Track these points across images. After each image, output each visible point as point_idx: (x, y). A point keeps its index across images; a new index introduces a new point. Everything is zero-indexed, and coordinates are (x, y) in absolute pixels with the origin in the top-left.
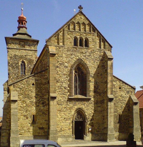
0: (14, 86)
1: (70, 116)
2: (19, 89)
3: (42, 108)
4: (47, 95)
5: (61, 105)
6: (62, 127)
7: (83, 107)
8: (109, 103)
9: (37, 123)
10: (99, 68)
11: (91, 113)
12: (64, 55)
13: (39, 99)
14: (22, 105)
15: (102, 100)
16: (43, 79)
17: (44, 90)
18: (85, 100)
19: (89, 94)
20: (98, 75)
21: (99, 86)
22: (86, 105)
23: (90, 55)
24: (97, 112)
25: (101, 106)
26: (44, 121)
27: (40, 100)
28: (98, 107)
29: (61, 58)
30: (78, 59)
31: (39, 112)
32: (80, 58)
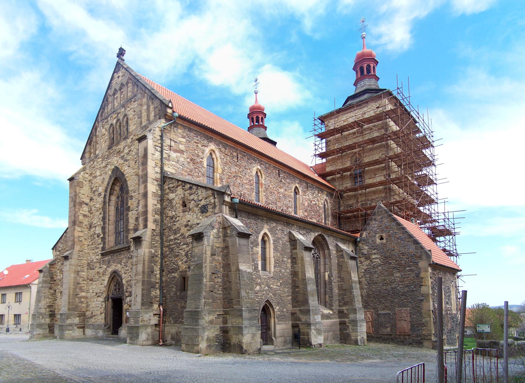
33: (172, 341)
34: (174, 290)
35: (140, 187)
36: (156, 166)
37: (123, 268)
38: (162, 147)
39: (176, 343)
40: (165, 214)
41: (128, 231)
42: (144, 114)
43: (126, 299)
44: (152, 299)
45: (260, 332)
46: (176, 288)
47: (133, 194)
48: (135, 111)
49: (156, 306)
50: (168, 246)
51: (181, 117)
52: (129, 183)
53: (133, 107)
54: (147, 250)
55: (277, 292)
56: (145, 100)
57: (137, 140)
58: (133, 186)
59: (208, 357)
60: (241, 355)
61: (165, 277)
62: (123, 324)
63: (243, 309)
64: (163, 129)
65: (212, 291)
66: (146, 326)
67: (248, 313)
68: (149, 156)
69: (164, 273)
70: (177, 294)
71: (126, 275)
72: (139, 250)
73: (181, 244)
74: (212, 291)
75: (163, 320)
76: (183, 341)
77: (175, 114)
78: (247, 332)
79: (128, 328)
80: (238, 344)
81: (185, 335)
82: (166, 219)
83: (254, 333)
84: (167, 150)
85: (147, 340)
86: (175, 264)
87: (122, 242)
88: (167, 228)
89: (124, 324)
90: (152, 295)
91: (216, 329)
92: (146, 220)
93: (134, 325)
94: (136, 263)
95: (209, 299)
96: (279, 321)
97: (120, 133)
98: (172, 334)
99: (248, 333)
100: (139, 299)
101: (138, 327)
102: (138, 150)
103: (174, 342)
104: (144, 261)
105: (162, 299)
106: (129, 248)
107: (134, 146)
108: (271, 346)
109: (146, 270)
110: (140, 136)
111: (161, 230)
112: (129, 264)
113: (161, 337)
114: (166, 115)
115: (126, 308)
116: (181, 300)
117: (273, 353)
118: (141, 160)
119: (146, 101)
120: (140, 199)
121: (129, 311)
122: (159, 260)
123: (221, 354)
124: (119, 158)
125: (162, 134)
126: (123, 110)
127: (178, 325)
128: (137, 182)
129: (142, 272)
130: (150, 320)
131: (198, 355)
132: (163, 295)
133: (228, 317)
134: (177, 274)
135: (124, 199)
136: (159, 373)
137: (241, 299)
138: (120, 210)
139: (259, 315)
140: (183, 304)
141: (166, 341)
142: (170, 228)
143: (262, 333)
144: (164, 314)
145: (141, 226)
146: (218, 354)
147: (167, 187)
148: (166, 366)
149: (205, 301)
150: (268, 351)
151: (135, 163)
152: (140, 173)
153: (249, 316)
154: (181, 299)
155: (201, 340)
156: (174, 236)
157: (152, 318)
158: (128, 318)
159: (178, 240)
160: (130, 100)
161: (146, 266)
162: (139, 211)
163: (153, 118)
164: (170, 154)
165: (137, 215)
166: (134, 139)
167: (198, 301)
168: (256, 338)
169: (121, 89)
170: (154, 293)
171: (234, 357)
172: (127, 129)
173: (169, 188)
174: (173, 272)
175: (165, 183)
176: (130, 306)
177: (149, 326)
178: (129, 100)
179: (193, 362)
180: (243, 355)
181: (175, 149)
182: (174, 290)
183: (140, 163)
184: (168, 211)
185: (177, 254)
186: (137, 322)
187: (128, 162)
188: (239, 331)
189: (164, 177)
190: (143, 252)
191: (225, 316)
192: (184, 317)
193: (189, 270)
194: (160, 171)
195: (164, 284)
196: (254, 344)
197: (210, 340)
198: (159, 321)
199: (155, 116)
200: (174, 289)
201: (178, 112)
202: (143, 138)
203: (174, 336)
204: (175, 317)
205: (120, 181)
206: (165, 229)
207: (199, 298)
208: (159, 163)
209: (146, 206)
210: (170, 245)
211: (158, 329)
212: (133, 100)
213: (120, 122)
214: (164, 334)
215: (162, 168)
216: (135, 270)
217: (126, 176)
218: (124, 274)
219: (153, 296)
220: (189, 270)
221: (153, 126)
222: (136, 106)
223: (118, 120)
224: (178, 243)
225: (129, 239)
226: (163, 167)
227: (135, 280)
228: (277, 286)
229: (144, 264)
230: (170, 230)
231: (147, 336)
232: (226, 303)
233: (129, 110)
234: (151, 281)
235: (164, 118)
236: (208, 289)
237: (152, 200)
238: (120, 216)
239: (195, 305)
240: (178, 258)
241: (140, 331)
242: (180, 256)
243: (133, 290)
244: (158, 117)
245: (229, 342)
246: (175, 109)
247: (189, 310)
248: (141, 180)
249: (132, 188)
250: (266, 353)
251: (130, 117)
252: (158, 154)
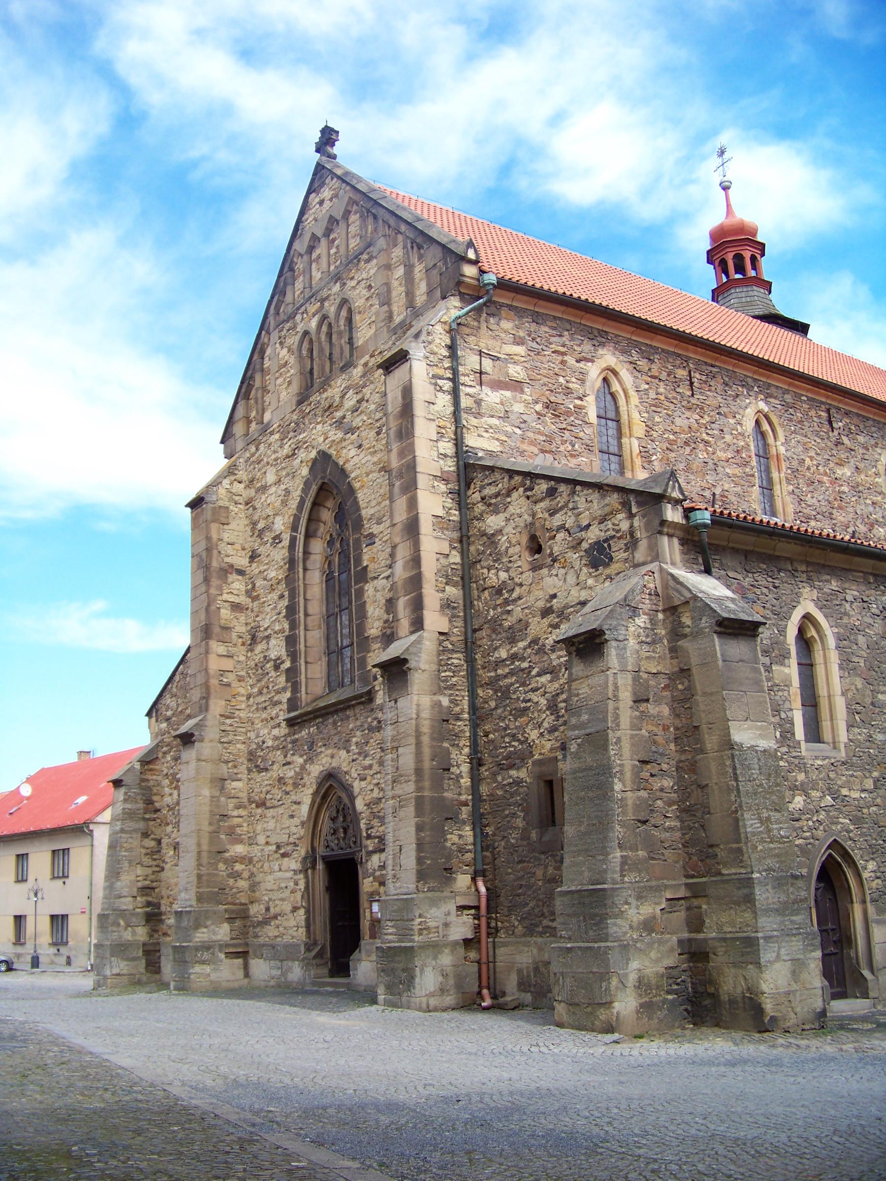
33: (523, 994)
34: (521, 825)
35: (394, 505)
36: (441, 435)
37: (353, 761)
38: (454, 380)
39: (535, 998)
40: (476, 582)
41: (364, 643)
42: (398, 292)
43: (367, 861)
44: (449, 857)
45: (818, 954)
46: (524, 819)
47: (376, 529)
48: (370, 287)
49: (463, 880)
50: (492, 683)
51: (504, 285)
52: (360, 495)
53: (364, 276)
54: (426, 701)
55: (865, 811)
56: (398, 252)
57: (379, 366)
58: (374, 503)
59: (644, 1042)
60: (757, 1035)
61: (488, 784)
62: (362, 942)
63: (756, 875)
64: (454, 326)
65: (645, 822)
66: (435, 947)
67: (773, 888)
68: (419, 410)
69: (483, 769)
70: (529, 838)
71: (363, 784)
72: (401, 703)
73: (534, 672)
74: (645, 822)
75: (488, 924)
76: (560, 992)
77: (486, 276)
78: (774, 955)
79: (379, 954)
80: (744, 997)
81: (562, 974)
82: (479, 597)
83: (797, 957)
84: (470, 386)
85: (442, 991)
86: (519, 740)
87: (347, 680)
88: (486, 626)
89: (366, 941)
90: (448, 844)
91: (665, 948)
92: (418, 605)
93: (396, 944)
94: (395, 744)
95: (637, 850)
96: (880, 911)
97: (331, 354)
98: (519, 971)
99: (778, 956)
100: (409, 860)
101: (409, 951)
102: (385, 395)
103: (528, 998)
104: (418, 734)
105: (484, 857)
106: (369, 697)
107: (372, 386)
108: (858, 1001)
109: (427, 765)
110: (388, 355)
111: (466, 634)
112: (372, 749)
113: (484, 983)
114: (459, 283)
115: (370, 890)
116: (543, 857)
117: (870, 1026)
118: (393, 424)
119: (401, 254)
120: (397, 540)
121: (378, 901)
122: (467, 729)
123: (687, 1032)
124: (331, 425)
125: (453, 340)
126: (337, 288)
127: (540, 940)
128: (385, 489)
129: (412, 771)
130: (446, 925)
131: (609, 1037)
132: (484, 843)
133: (704, 907)
134: (524, 770)
135: (348, 545)
136: (487, 1099)
137: (746, 843)
138: (339, 581)
139: (809, 894)
140: (550, 870)
141: (504, 994)
142: (495, 625)
143: (824, 955)
144: (493, 904)
145: (404, 624)
146: (679, 1030)
147: (477, 496)
148: (506, 1075)
149: (622, 856)
150: (851, 1018)
151: (378, 433)
152: (395, 463)
153: (776, 900)
154: (543, 853)
155: (617, 988)
156: (508, 647)
157: (453, 918)
158: (379, 921)
159: (523, 659)
160: (356, 257)
161: (427, 752)
162: (396, 579)
163: (424, 297)
164: (480, 397)
165: (390, 590)
166: (370, 364)
167: (601, 857)
168: (804, 976)
169: (328, 232)
170: (455, 839)
171: (736, 1044)
172: (351, 339)
173: (483, 499)
174: (512, 767)
175: (472, 486)
176: (382, 884)
177: (445, 946)
178: (354, 260)
179: (595, 1060)
180: (766, 1035)
181: (496, 377)
182: (521, 825)
183: (392, 433)
184: (485, 571)
185: (522, 705)
186: (405, 933)
187: (357, 434)
188: (748, 953)
189: (467, 466)
190: (414, 707)
191: (695, 902)
192: (557, 912)
193: (565, 757)
194: (454, 450)
195: (486, 808)
196: (801, 995)
197: (649, 986)
198: (477, 928)
199: (430, 292)
200: (519, 822)
201: (494, 270)
202: (398, 358)
203: (529, 976)
204: (529, 913)
205: (335, 493)
206: (480, 629)
207: (604, 848)
208: (449, 426)
209: (416, 561)
210: (498, 678)
211: (473, 955)
212: (365, 256)
213: (330, 324)
214: (495, 973)
215: (458, 442)
216: (393, 766)
217: (353, 475)
218: (357, 781)
219: (454, 848)
220: (565, 757)
221: (426, 322)
222: (372, 272)
223: (324, 317)
224: (523, 670)
225: (369, 668)
226: (462, 438)
227: (393, 798)
228: (863, 791)
229: (418, 744)
230: (494, 631)
231: (440, 979)
232: (695, 858)
233: (353, 287)
234: (443, 799)
235: (457, 293)
236: (630, 814)
237: (435, 542)
238: (340, 599)
239: (590, 870)
240: (525, 719)
241: (418, 962)
242: (533, 713)
243: (389, 830)
244: (438, 293)
245: (711, 990)
246: (486, 264)
247: (573, 888)
248: (398, 484)
249: (372, 511)
250: (844, 1025)
251: (357, 304)
252: (444, 402)
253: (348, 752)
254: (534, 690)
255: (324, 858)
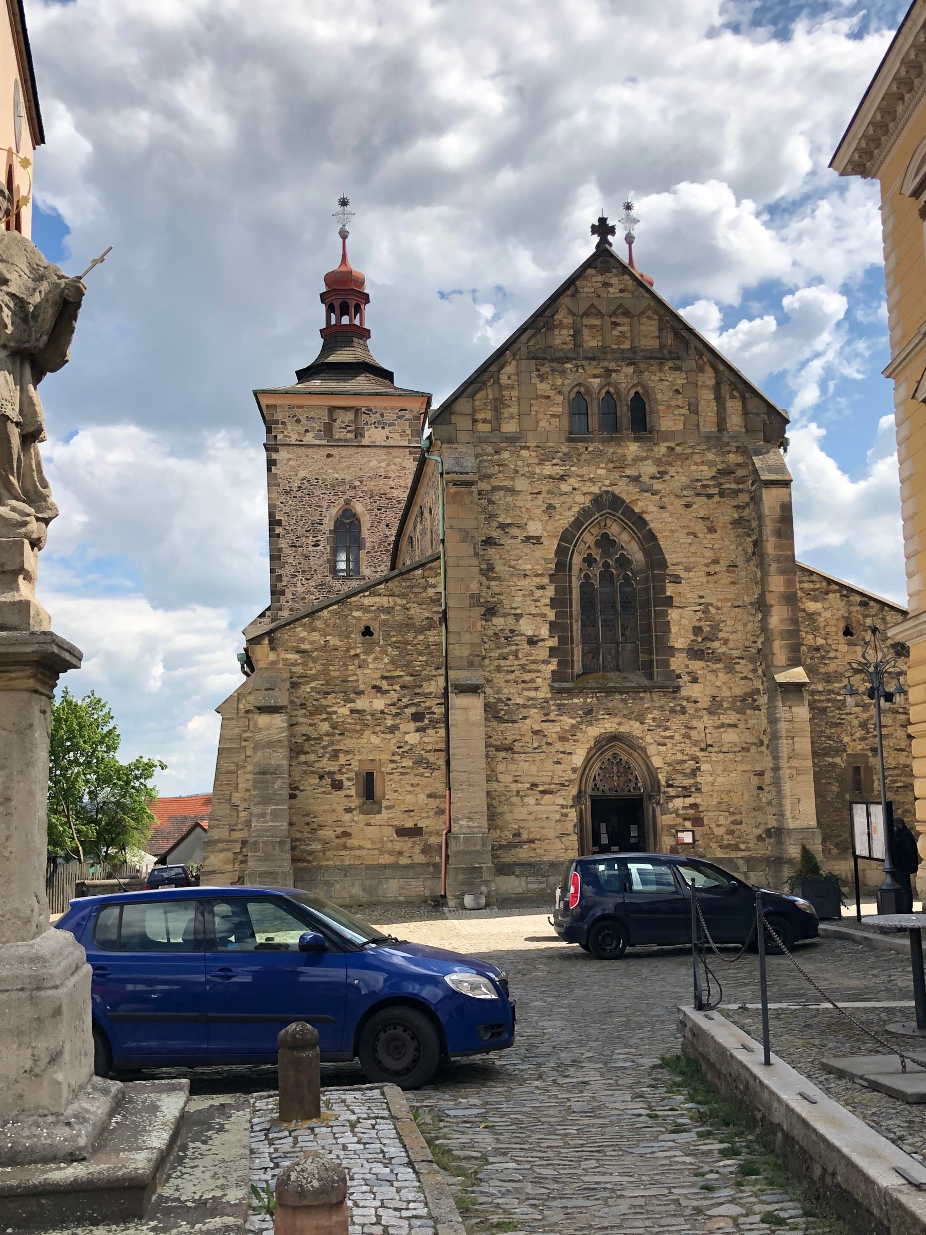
0: (271, 642)
1: (564, 773)
2: (297, 656)
3: (413, 738)
4: (436, 676)
5: (514, 722)
6: (523, 824)
7: (634, 728)
8: (782, 712)
9: (387, 808)
10: (717, 536)
11: (679, 757)
12: (521, 484)
13: (395, 700)
14: (311, 725)
15: (746, 694)
16: (415, 605)
17: (420, 654)
18: (642, 695)
19: (667, 664)
20: (711, 569)
21: (722, 625)
22: (654, 719)
23: (662, 469)
24: (717, 753)
25: (742, 726)
26: (422, 797)
27: (404, 700)
28: (722, 730)
29: (509, 499)
30: (598, 500)
31: (396, 758)
32: (607, 492)
86: (835, 741)
156: (825, 684)
159: (839, 694)
174: (827, 754)
253: (642, 723)
254: (846, 714)
255: (591, 796)
